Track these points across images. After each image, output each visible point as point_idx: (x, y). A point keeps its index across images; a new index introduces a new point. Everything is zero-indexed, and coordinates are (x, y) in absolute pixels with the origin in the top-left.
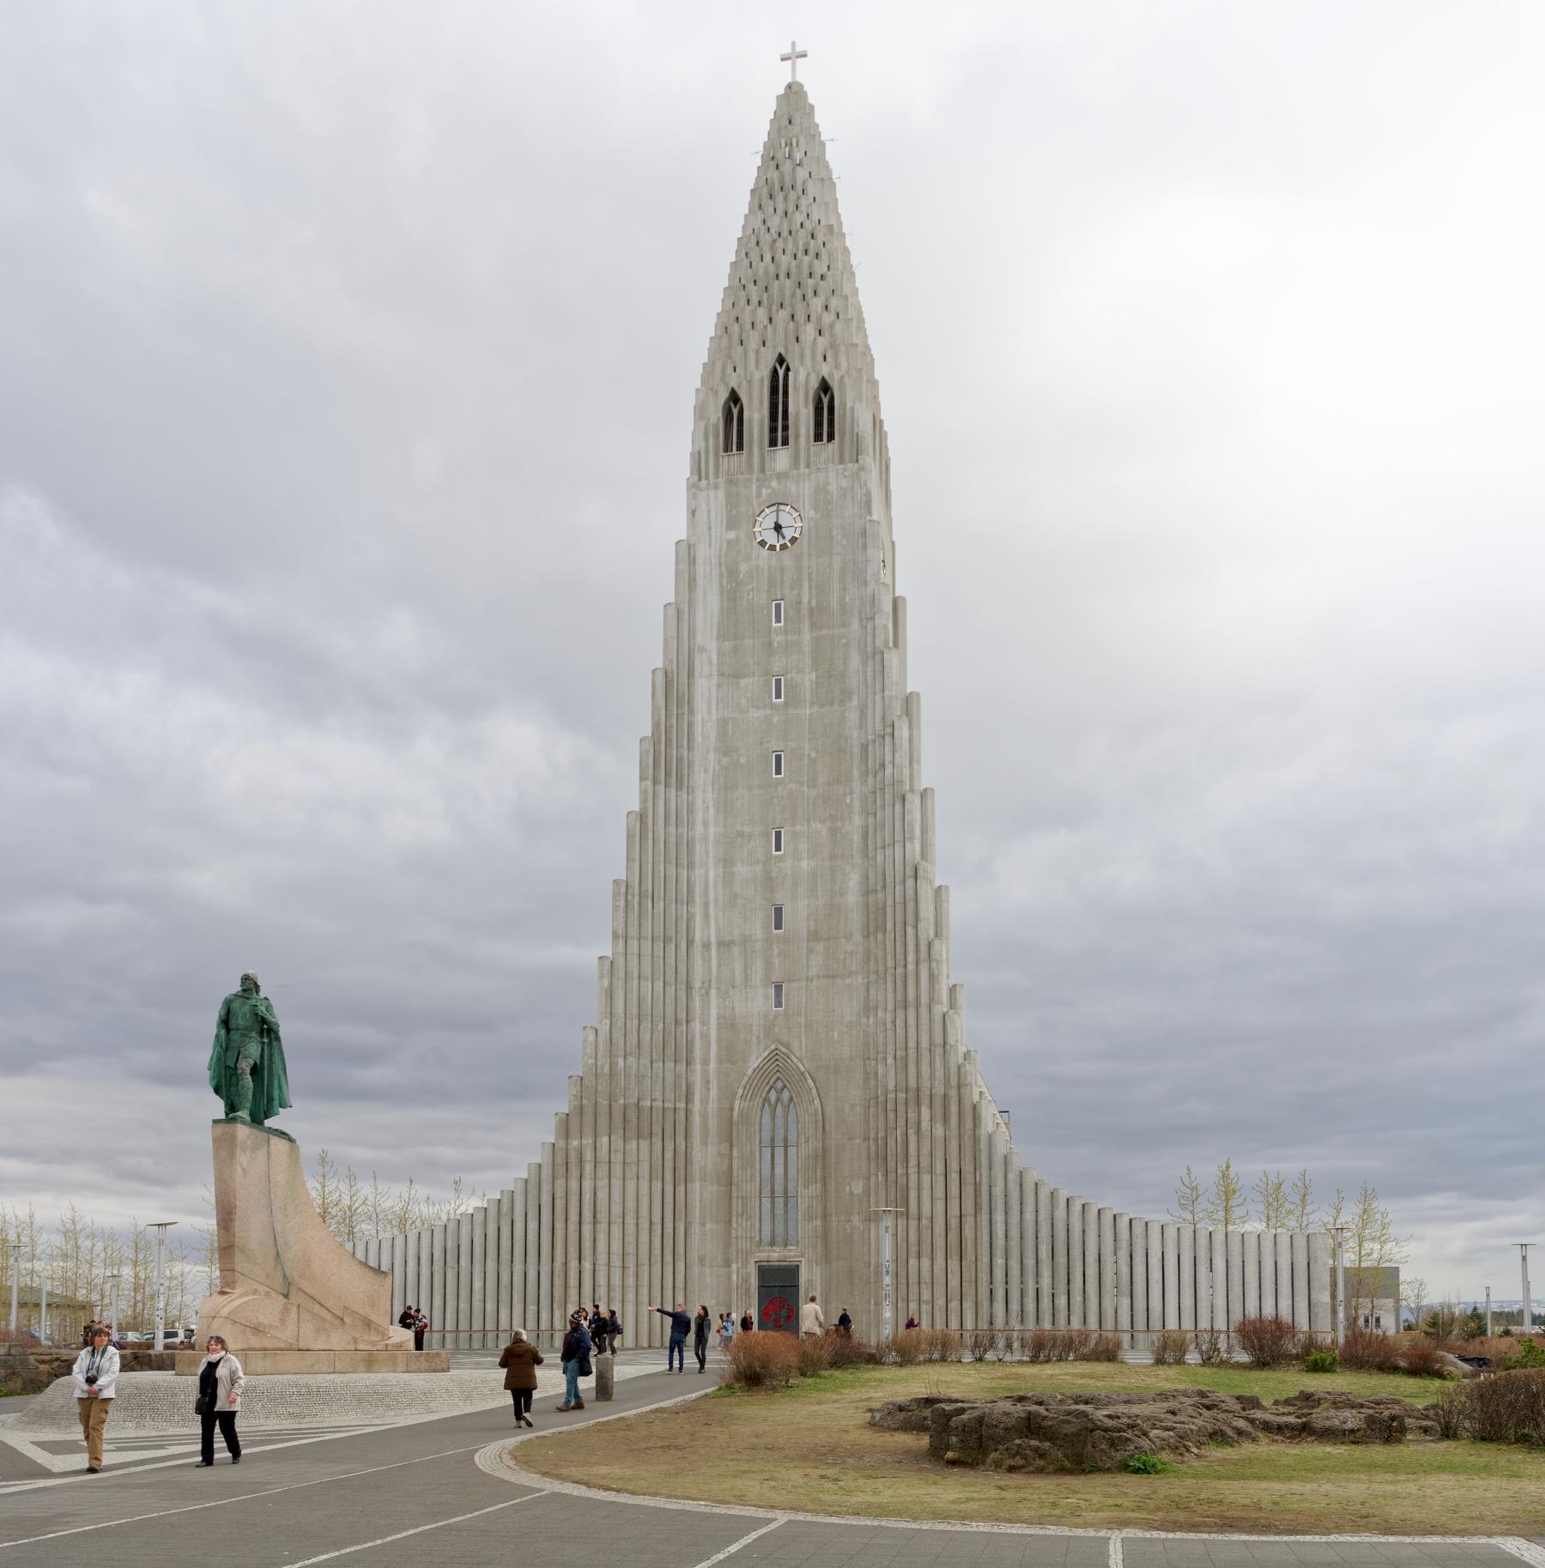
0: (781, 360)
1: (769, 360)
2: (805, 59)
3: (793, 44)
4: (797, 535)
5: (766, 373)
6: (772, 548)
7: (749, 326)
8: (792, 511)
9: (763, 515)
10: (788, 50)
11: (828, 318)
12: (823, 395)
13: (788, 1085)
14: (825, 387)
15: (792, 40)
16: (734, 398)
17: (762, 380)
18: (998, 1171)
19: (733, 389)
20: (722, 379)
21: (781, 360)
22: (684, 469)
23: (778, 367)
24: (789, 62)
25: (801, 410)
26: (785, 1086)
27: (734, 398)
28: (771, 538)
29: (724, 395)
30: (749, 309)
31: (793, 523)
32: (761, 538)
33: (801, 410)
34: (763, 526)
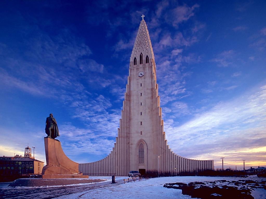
0: (141, 53)
1: (139, 54)
5: (139, 56)
6: (140, 77)
14: (147, 56)
16: (135, 58)
20: (134, 56)
25: (144, 59)
27: (135, 58)
33: (144, 59)
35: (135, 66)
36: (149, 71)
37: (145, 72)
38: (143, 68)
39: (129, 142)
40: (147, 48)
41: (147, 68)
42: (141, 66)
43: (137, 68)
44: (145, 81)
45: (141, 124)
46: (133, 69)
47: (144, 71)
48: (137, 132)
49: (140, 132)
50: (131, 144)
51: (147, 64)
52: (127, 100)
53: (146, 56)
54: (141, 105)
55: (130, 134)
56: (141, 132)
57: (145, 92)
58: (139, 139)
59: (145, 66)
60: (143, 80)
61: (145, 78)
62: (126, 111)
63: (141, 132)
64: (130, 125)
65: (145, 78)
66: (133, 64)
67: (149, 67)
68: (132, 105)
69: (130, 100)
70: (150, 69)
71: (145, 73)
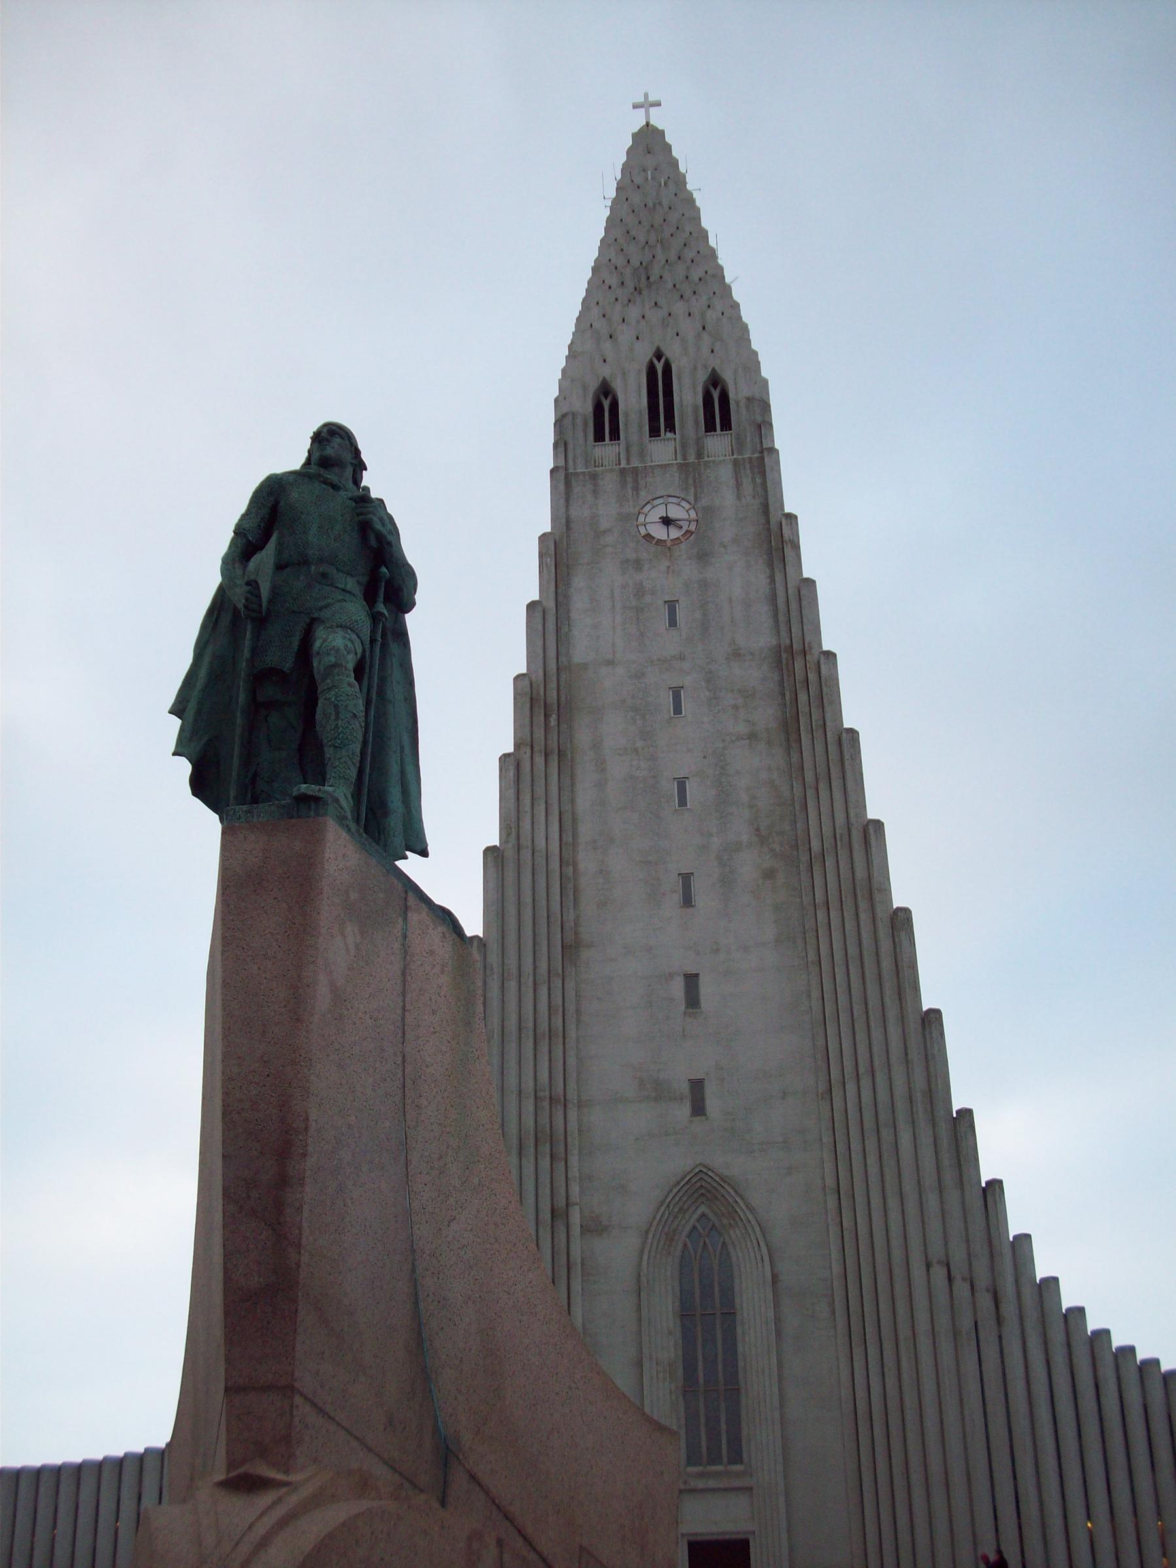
0: (659, 355)
1: (644, 353)
2: (660, 107)
3: (646, 96)
4: (693, 527)
6: (659, 542)
7: (617, 318)
8: (684, 504)
9: (648, 507)
10: (642, 100)
11: (711, 315)
12: (712, 389)
13: (717, 1223)
14: (715, 380)
15: (644, 92)
16: (605, 390)
17: (639, 371)
18: (1057, 1337)
19: (604, 379)
21: (659, 355)
22: (546, 460)
23: (656, 361)
24: (643, 110)
26: (713, 1226)
27: (605, 390)
28: (659, 532)
29: (593, 385)
30: (618, 307)
31: (687, 517)
32: (646, 533)
34: (647, 520)
35: (607, 451)
36: (739, 498)
37: (704, 502)
38: (684, 467)
39: (561, 1203)
40: (703, 315)
41: (725, 473)
42: (663, 451)
43: (623, 464)
44: (704, 584)
45: (693, 1000)
46: (594, 477)
47: (691, 499)
48: (658, 1092)
49: (685, 1088)
50: (585, 1230)
51: (718, 444)
52: (539, 746)
53: (702, 377)
54: (683, 802)
55: (573, 1115)
56: (697, 1086)
57: (710, 678)
58: (679, 1162)
59: (699, 455)
60: (689, 570)
61: (703, 557)
62: (526, 855)
63: (697, 1086)
64: (571, 1008)
65: (703, 557)
66: (591, 436)
67: (736, 463)
68: (585, 798)
69: (561, 754)
70: (746, 482)
71: (707, 515)
